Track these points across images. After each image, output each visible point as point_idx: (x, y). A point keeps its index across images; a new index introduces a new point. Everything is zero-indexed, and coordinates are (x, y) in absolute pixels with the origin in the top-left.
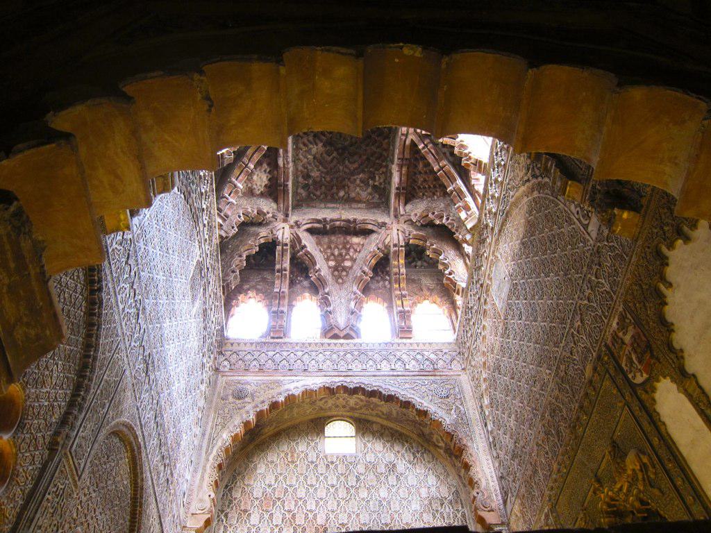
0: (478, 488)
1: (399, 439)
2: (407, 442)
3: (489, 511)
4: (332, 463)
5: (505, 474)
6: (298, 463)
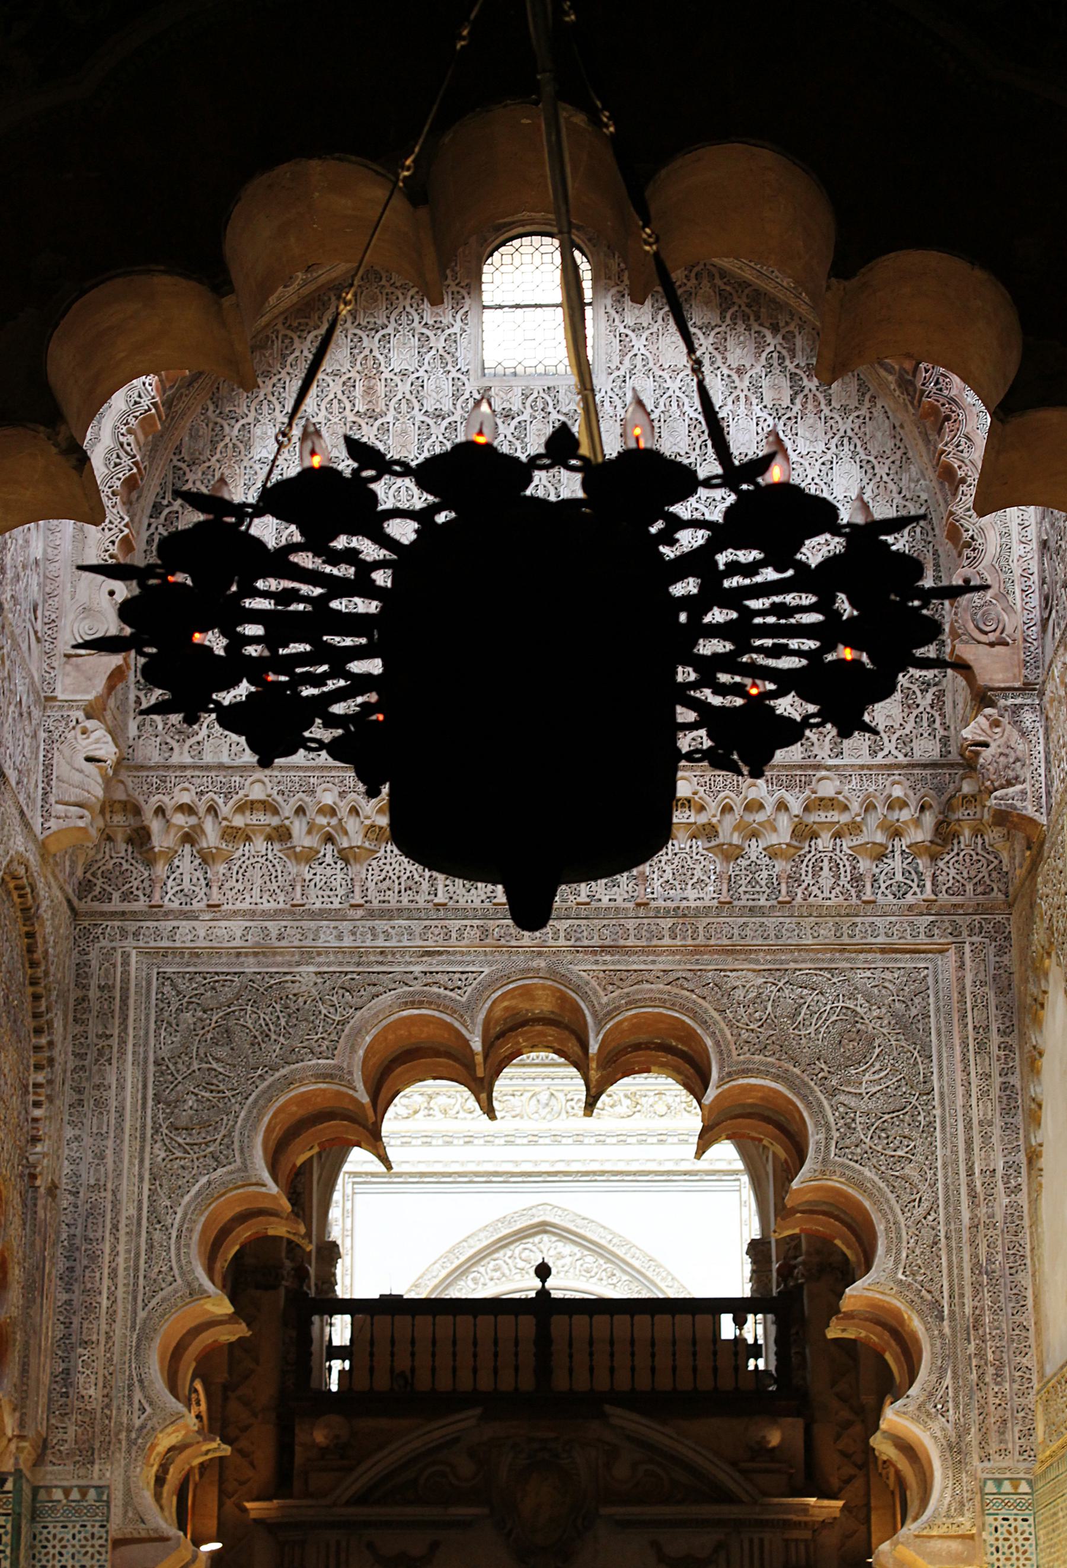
0: (973, 561)
1: (746, 318)
2: (775, 329)
3: (992, 645)
4: (508, 415)
5: (1052, 544)
6: (389, 418)
